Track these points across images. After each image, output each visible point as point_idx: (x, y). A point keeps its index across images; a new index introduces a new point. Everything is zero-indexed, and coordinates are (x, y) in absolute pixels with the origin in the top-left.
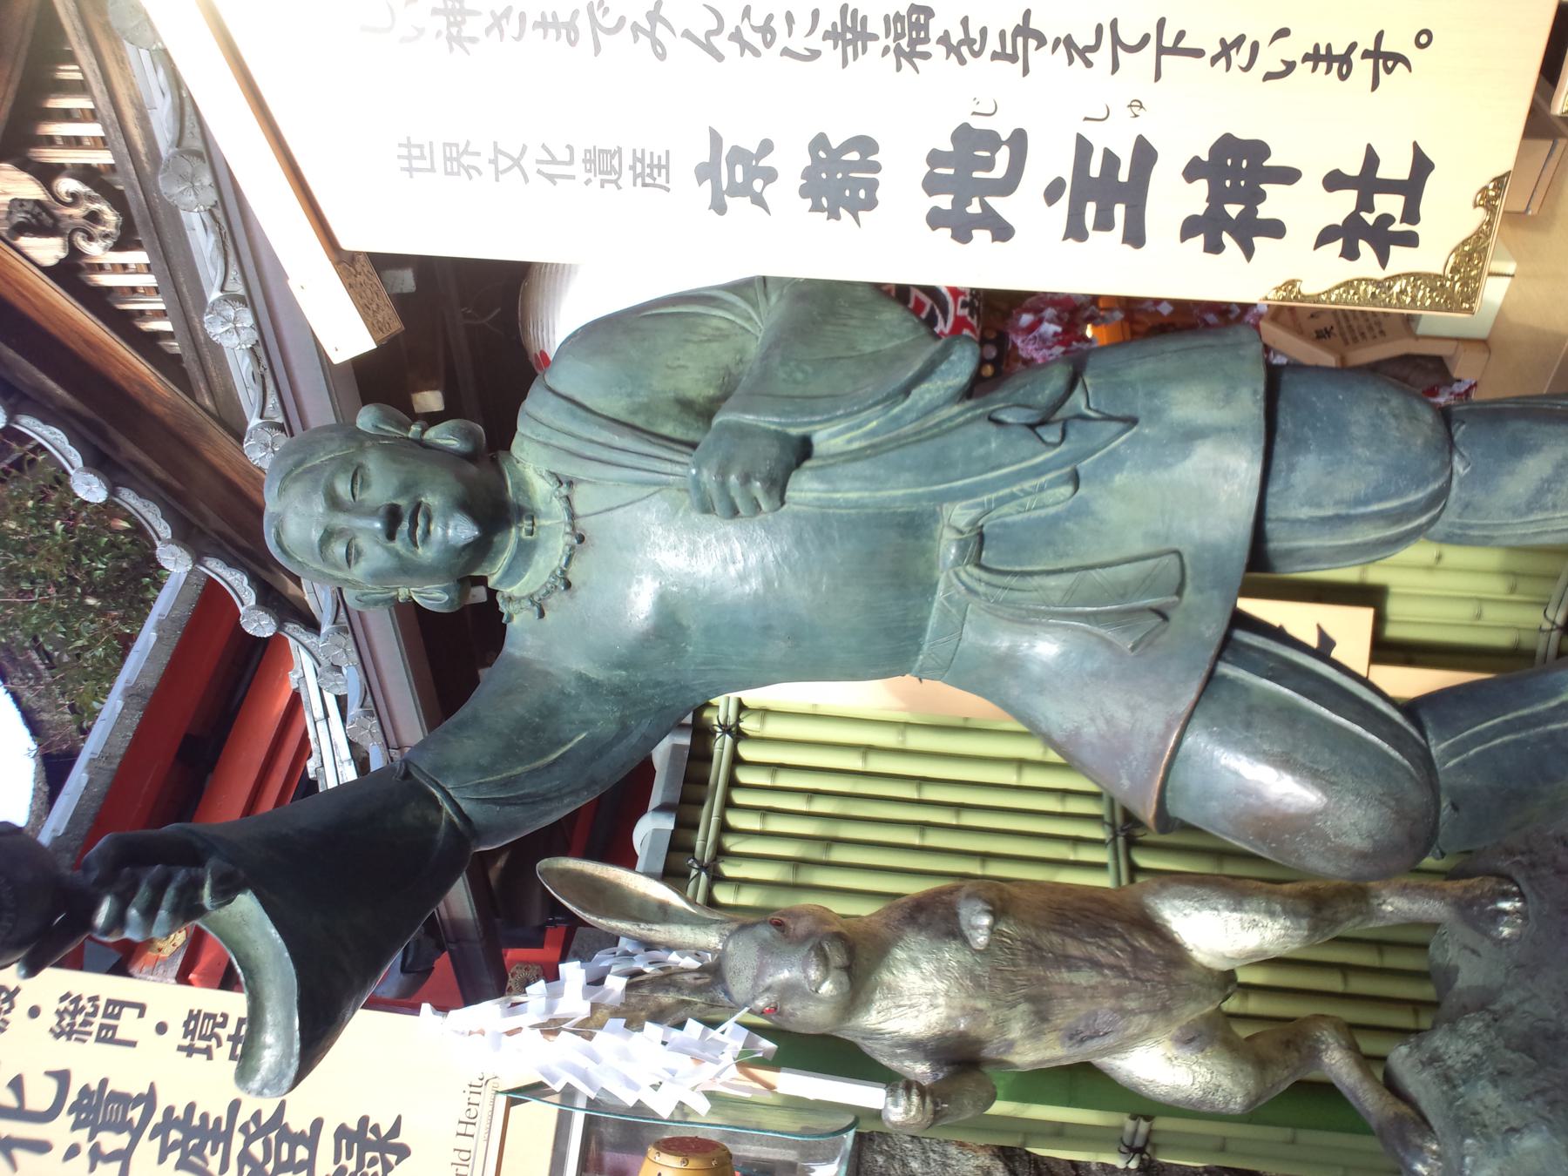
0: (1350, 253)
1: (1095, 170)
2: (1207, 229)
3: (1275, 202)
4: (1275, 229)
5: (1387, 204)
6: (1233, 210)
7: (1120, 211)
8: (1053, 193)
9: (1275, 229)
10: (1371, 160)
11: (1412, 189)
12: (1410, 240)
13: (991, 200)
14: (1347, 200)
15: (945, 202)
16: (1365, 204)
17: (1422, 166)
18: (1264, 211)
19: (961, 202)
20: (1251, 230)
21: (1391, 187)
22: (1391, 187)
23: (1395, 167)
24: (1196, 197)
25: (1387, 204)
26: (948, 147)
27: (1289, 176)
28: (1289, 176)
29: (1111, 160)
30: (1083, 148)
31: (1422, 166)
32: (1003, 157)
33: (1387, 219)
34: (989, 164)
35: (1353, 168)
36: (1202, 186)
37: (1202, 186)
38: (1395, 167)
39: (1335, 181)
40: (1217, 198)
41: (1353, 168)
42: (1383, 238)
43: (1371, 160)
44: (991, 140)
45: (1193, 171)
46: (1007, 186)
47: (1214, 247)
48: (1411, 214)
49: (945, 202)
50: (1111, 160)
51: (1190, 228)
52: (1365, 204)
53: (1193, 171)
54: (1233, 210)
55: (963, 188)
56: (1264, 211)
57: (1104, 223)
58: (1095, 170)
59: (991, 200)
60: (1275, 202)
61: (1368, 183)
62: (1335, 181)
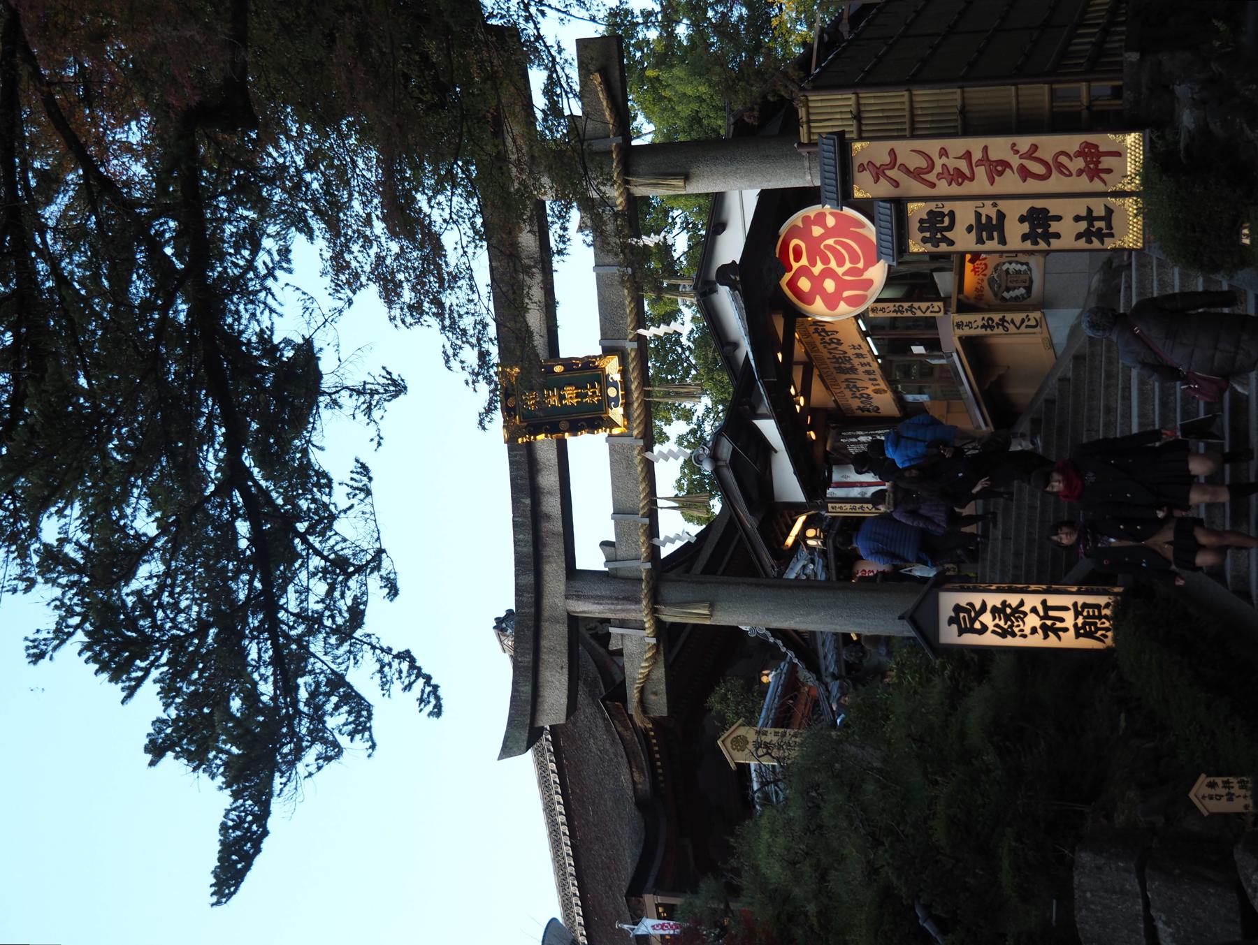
1: (984, 221)
3: (1054, 227)
4: (1057, 236)
5: (1098, 224)
6: (1040, 231)
7: (995, 234)
8: (970, 229)
9: (1057, 236)
10: (1090, 211)
12: (1112, 235)
13: (947, 234)
14: (1083, 225)
16: (1091, 225)
18: (1051, 230)
20: (1048, 236)
21: (1100, 219)
22: (1100, 219)
23: (1099, 211)
24: (1026, 228)
25: (1098, 224)
26: (925, 217)
27: (1059, 218)
28: (1059, 218)
30: (978, 215)
31: (1109, 211)
32: (947, 220)
33: (1100, 229)
34: (942, 222)
35: (1084, 213)
36: (1026, 225)
37: (1026, 225)
39: (1077, 219)
40: (1033, 228)
41: (1084, 213)
42: (1101, 236)
43: (1090, 211)
44: (942, 215)
45: (1022, 219)
46: (951, 227)
48: (1110, 227)
51: (1025, 237)
52: (1091, 225)
53: (1022, 219)
54: (1040, 231)
56: (1051, 230)
57: (991, 238)
58: (984, 221)
59: (947, 234)
60: (1054, 227)
61: (1090, 217)
62: (1077, 219)
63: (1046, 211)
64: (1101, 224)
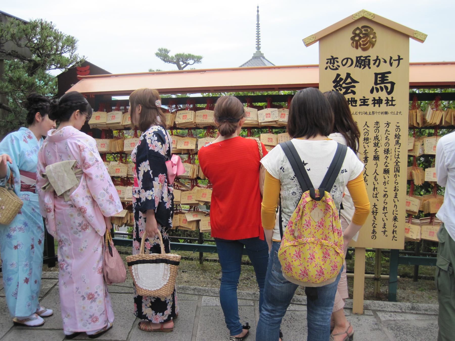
0: (386, 100)
2: (374, 99)
11: (392, 105)
15: (350, 100)
17: (394, 105)
19: (350, 101)
21: (392, 103)
22: (392, 103)
23: (394, 103)
25: (390, 103)
29: (367, 102)
38: (394, 103)
47: (372, 100)
49: (350, 100)
50: (367, 102)
54: (376, 102)
55: (351, 101)
63: (382, 103)
64: (390, 103)
